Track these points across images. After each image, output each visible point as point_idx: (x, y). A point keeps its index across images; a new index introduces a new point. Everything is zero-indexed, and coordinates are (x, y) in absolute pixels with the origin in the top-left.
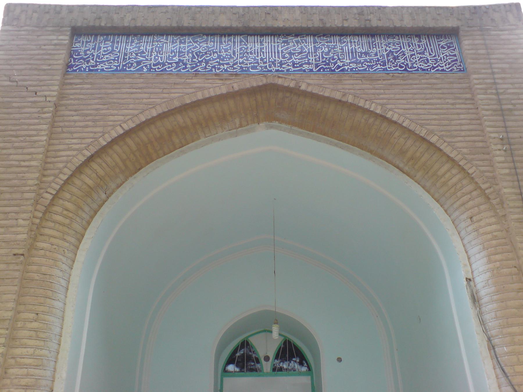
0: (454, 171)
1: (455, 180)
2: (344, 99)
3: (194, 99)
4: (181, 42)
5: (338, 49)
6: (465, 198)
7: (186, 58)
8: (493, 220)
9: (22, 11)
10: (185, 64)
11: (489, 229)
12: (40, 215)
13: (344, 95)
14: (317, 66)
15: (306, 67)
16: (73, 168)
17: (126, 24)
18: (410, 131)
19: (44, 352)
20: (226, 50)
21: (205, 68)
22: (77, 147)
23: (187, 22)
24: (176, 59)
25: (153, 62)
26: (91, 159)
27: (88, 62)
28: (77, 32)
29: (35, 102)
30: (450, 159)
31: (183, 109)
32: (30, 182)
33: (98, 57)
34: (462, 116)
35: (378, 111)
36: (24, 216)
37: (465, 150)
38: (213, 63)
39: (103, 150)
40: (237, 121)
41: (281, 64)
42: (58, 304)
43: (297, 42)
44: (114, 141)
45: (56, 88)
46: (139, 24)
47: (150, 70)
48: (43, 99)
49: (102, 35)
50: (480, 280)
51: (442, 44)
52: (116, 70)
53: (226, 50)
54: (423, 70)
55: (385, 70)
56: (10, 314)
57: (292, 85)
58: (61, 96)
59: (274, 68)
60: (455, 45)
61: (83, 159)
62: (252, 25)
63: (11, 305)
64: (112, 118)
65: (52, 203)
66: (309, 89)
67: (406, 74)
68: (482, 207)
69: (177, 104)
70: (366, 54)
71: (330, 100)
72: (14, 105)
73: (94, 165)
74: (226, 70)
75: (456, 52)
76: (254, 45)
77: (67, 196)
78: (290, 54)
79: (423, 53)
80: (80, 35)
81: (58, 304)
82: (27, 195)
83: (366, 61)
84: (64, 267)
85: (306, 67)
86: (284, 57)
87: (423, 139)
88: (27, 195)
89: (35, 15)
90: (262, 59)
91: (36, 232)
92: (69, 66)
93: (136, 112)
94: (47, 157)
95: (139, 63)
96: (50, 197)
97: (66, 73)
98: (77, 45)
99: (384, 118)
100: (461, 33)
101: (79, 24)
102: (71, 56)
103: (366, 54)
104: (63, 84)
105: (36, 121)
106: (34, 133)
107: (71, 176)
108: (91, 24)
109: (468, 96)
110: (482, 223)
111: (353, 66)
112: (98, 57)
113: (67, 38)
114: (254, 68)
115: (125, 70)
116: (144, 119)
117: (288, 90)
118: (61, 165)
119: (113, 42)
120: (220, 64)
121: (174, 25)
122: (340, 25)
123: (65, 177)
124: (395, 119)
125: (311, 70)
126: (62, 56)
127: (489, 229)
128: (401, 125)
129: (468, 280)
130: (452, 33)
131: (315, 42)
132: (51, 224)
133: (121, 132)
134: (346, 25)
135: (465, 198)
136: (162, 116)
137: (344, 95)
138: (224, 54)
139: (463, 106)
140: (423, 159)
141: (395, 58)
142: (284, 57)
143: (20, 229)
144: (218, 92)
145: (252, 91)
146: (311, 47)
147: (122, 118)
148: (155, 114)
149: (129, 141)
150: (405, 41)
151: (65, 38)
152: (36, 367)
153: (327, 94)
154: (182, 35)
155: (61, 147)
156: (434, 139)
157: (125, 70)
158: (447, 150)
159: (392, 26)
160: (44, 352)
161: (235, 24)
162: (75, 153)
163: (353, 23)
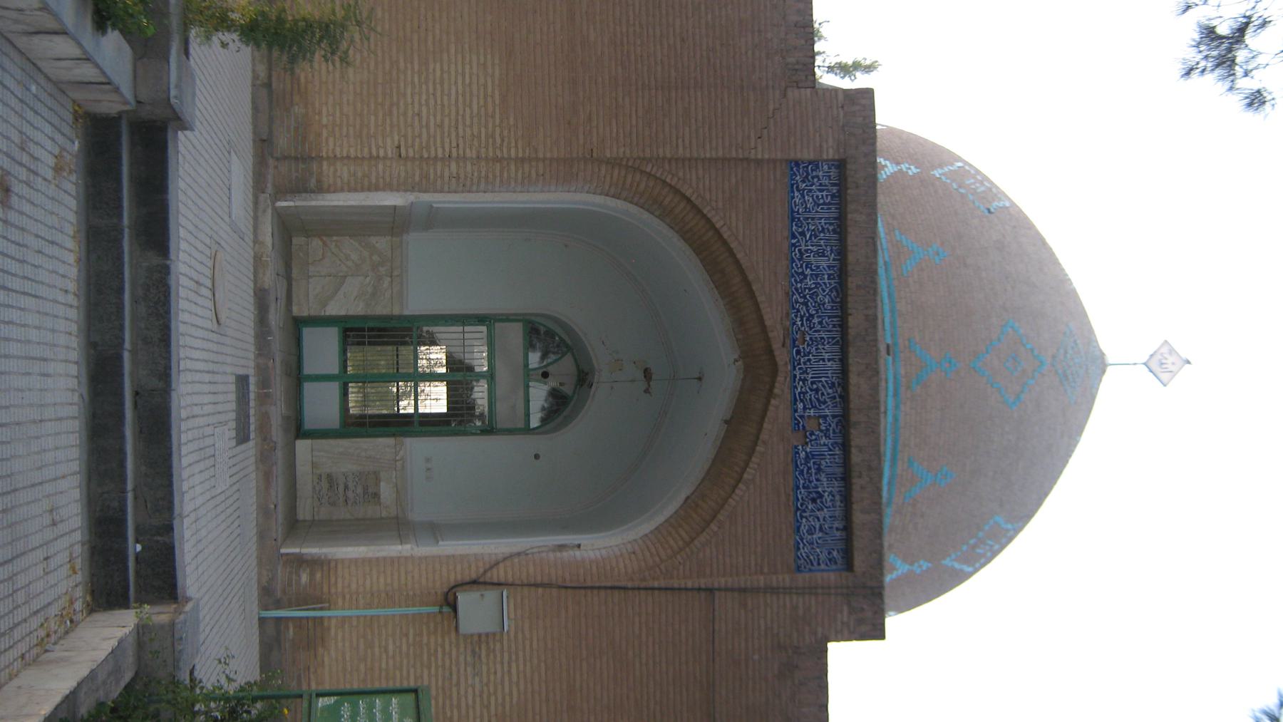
0: (681, 543)
1: (672, 542)
2: (760, 442)
3: (757, 294)
4: (829, 275)
5: (824, 440)
6: (653, 550)
7: (810, 282)
8: (630, 570)
9: (864, 106)
10: (801, 282)
11: (621, 565)
12: (630, 164)
13: (764, 442)
14: (801, 417)
15: (800, 406)
16: (678, 187)
17: (849, 216)
18: (723, 505)
19: (513, 184)
20: (820, 323)
21: (797, 302)
22: (701, 186)
23: (853, 282)
24: (808, 272)
25: (803, 248)
26: (689, 200)
27: (803, 181)
28: (841, 165)
29: (749, 137)
30: (693, 540)
31: (747, 284)
32: (661, 151)
33: (810, 191)
34: (741, 559)
35: (745, 476)
36: (628, 152)
37: (701, 555)
38: (803, 310)
39: (699, 211)
40: (740, 336)
42: (553, 188)
43: (834, 398)
44: (708, 221)
45: (766, 156)
46: (850, 229)
47: (793, 245)
48: (753, 145)
49: (838, 191)
51: (835, 553)
52: (793, 211)
54: (798, 528)
55: (798, 488)
56: (541, 156)
57: (776, 391)
58: (759, 162)
59: (797, 373)
60: (834, 567)
61: (688, 194)
62: (851, 349)
63: (548, 155)
64: (734, 215)
65: (642, 172)
66: (771, 408)
67: (793, 509)
68: (643, 564)
69: (751, 277)
70: (819, 470)
71: (760, 430)
72: (746, 120)
73: (682, 205)
74: (794, 324)
75: (823, 566)
76: (827, 351)
77: (651, 184)
78: (817, 390)
79: (821, 530)
80: (838, 167)
81: (553, 188)
82: (648, 150)
83: (809, 468)
84: (586, 188)
85: (800, 406)
86: (812, 383)
87: (714, 517)
88: (648, 150)
89: (860, 120)
90: (809, 360)
91: (614, 163)
92: (797, 164)
93: (741, 238)
94: (690, 160)
95: (802, 234)
96: (648, 170)
97: (789, 162)
98: (826, 167)
99: (739, 480)
100: (845, 574)
101: (849, 166)
102: (810, 163)
103: (819, 470)
104: (775, 161)
105: (727, 144)
106: (714, 145)
107: (670, 185)
108: (849, 180)
109: (766, 570)
110: (627, 562)
111: (803, 455)
112: (810, 191)
113: (831, 157)
114: (798, 352)
115: (793, 221)
116: (732, 246)
117: (772, 387)
118: (681, 174)
119: (829, 204)
120: (802, 318)
121: (850, 268)
122: (852, 443)
123: (668, 180)
124: (737, 491)
125: (796, 411)
126: (807, 155)
127: (621, 565)
128: (730, 496)
131: (834, 417)
132: (623, 173)
133: (718, 226)
134: (853, 450)
135: (653, 550)
136: (737, 262)
137: (764, 442)
138: (816, 320)
139: (753, 563)
140: (694, 516)
141: (814, 500)
142: (812, 383)
143: (615, 150)
144: (766, 317)
145: (770, 352)
146: (827, 412)
147: (734, 225)
148: (739, 256)
149: (710, 233)
150: (838, 512)
151: (830, 154)
152: (501, 181)
153: (765, 425)
154: (840, 276)
155: (701, 172)
156: (714, 527)
157: (793, 221)
158: (703, 538)
159: (854, 500)
160: (513, 184)
161: (852, 332)
162: (694, 185)
163: (856, 457)
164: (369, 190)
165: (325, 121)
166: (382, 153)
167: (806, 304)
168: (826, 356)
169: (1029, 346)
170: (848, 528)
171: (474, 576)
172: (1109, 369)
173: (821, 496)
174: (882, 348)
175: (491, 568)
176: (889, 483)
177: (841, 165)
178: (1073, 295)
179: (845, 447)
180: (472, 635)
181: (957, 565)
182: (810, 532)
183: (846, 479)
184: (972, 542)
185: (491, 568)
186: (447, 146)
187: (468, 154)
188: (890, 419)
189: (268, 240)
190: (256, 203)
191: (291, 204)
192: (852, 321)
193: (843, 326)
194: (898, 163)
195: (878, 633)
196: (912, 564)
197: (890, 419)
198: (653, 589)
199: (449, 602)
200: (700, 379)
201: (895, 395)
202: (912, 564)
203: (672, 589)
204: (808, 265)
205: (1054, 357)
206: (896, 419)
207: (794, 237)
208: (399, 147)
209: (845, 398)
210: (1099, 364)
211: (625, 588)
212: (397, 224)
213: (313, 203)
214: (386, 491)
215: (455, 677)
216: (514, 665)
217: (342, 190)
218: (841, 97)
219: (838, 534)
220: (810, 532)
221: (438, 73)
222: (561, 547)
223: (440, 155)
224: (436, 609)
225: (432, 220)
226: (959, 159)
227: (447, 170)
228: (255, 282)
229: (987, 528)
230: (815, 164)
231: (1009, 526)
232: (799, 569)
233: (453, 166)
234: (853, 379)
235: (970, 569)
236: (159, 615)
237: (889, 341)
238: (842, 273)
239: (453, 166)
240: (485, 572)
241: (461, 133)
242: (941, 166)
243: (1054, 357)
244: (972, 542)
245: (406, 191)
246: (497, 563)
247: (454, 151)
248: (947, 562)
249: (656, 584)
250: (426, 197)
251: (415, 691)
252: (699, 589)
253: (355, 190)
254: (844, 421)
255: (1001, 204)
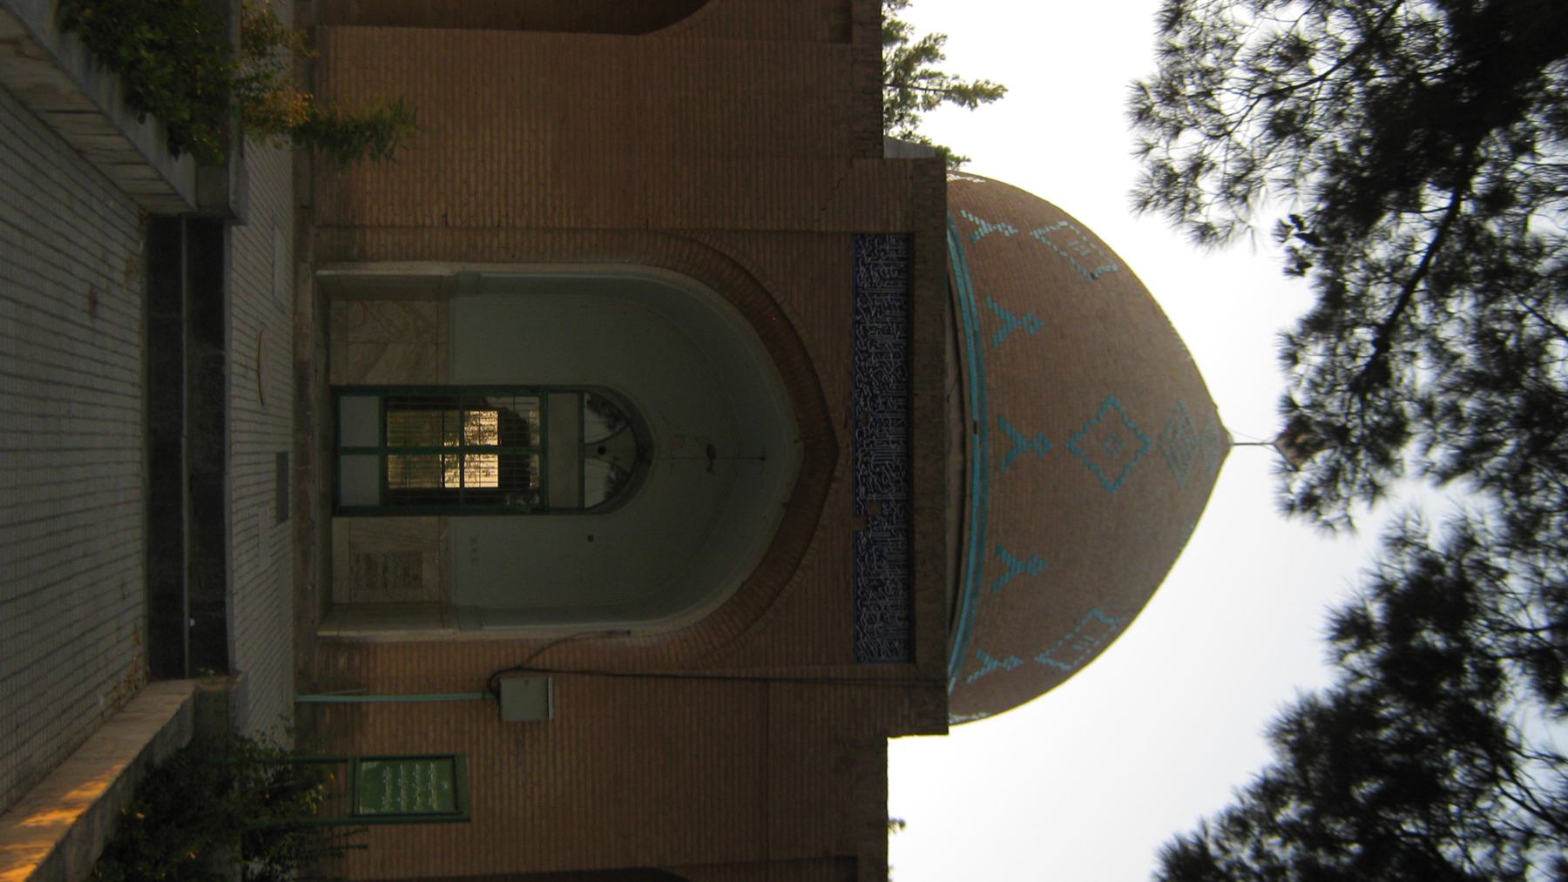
7: (874, 361)
14: (864, 501)
15: (862, 490)
20: (885, 403)
26: (748, 273)
28: (909, 238)
41: (867, 463)
47: (858, 322)
50: (627, 641)
53: (885, 403)
57: (837, 474)
70: (881, 557)
78: (880, 474)
85: (862, 490)
92: (863, 236)
95: (868, 310)
102: (877, 235)
111: (864, 541)
114: (861, 434)
129: (629, 633)
130: (911, 657)
134: (917, 536)
138: (880, 401)
141: (875, 589)
157: (857, 295)
163: (919, 544)
164: (415, 259)
165: (368, 188)
166: (428, 222)
167: (870, 384)
168: (891, 438)
169: (1131, 425)
170: (910, 618)
171: (518, 661)
172: (1235, 451)
173: (882, 584)
174: (969, 426)
175: (536, 654)
176: (976, 571)
177: (909, 238)
178: (1192, 365)
179: (909, 534)
180: (516, 723)
181: (1051, 662)
182: (871, 622)
183: (909, 566)
184: (1068, 637)
185: (536, 654)
186: (496, 215)
187: (518, 223)
188: (976, 503)
189: (309, 310)
190: (296, 272)
191: (333, 272)
192: (917, 402)
193: (908, 407)
194: (994, 223)
195: (945, 732)
196: (1001, 660)
197: (976, 503)
198: (705, 678)
199: (493, 689)
200: (763, 459)
201: (982, 477)
202: (1001, 660)
203: (724, 678)
204: (873, 343)
205: (1160, 437)
206: (982, 501)
207: (858, 313)
208: (445, 216)
209: (909, 481)
210: (1221, 444)
211: (675, 677)
212: (441, 290)
213: (356, 272)
214: (428, 573)
215: (497, 767)
216: (559, 755)
217: (386, 259)
218: (910, 166)
219: (900, 624)
220: (871, 622)
221: (488, 139)
222: (611, 634)
223: (488, 224)
224: (478, 696)
225: (479, 286)
226: (1066, 217)
227: (496, 241)
228: (295, 355)
229: (1084, 622)
230: (882, 237)
231: (1111, 621)
232: (858, 660)
233: (502, 236)
234: (918, 463)
235: (1068, 667)
236: (213, 684)
237: (976, 417)
238: (908, 352)
239: (502, 236)
240: (530, 658)
241: (511, 201)
242: (1041, 226)
243: (1160, 437)
244: (1068, 637)
245: (453, 260)
246: (542, 650)
247: (504, 221)
248: (1041, 659)
249: (708, 673)
250: (474, 267)
251: (452, 757)
252: (753, 679)
253: (400, 260)
254: (908, 505)
255: (1108, 268)
